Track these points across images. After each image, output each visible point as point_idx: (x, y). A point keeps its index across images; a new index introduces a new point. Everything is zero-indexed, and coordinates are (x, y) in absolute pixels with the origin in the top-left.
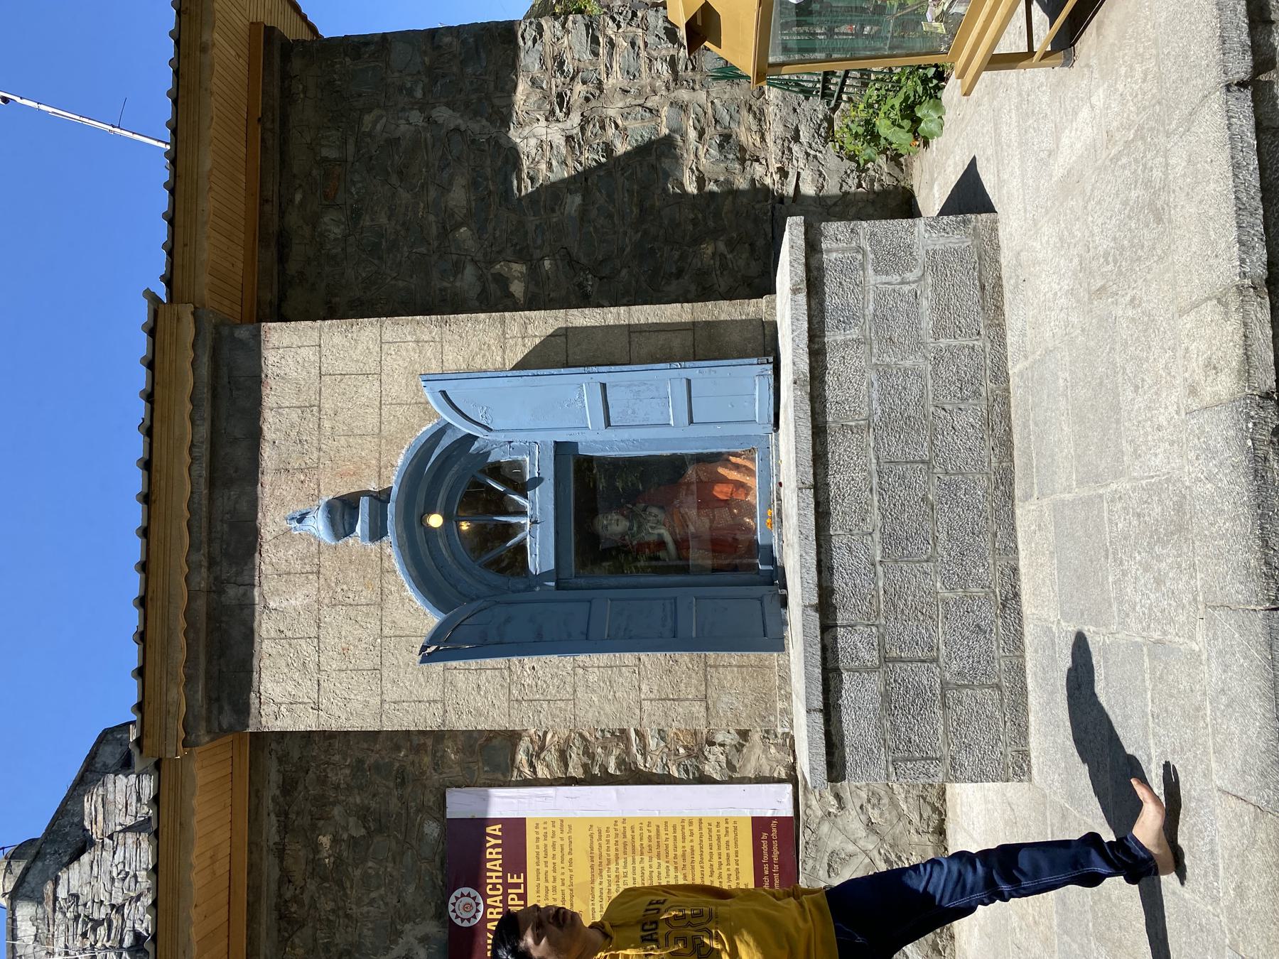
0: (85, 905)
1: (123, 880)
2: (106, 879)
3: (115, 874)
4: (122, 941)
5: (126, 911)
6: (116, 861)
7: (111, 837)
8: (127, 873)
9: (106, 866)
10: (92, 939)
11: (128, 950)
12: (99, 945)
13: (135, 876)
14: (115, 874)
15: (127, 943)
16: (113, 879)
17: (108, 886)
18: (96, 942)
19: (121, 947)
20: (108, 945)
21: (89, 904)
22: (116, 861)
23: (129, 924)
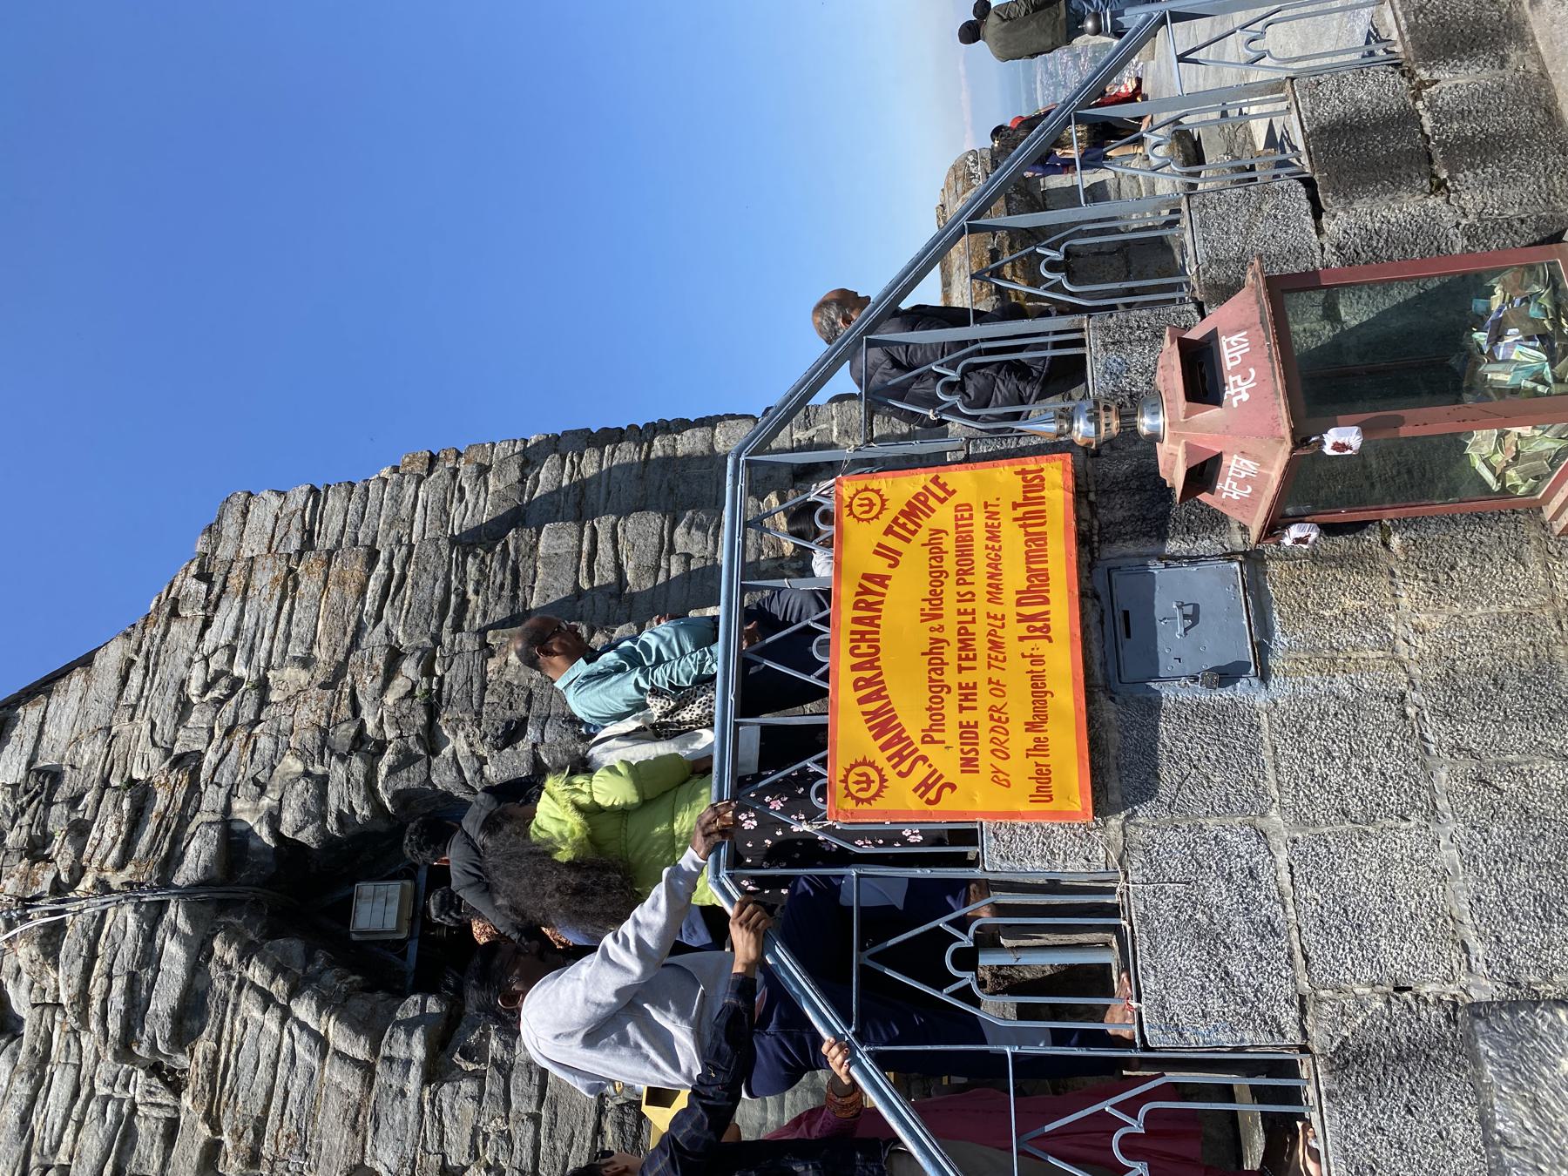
0: (74, 801)
1: (220, 702)
2: (162, 705)
3: (193, 689)
4: (172, 861)
5: (211, 757)
6: (208, 645)
7: (204, 576)
8: (236, 683)
9: (171, 669)
10: (62, 853)
11: (186, 893)
12: (87, 882)
13: (263, 686)
14: (193, 689)
15: (189, 870)
16: (184, 707)
17: (166, 730)
18: (78, 872)
19: (165, 883)
20: (116, 880)
21: (89, 798)
22: (208, 645)
23: (212, 799)
